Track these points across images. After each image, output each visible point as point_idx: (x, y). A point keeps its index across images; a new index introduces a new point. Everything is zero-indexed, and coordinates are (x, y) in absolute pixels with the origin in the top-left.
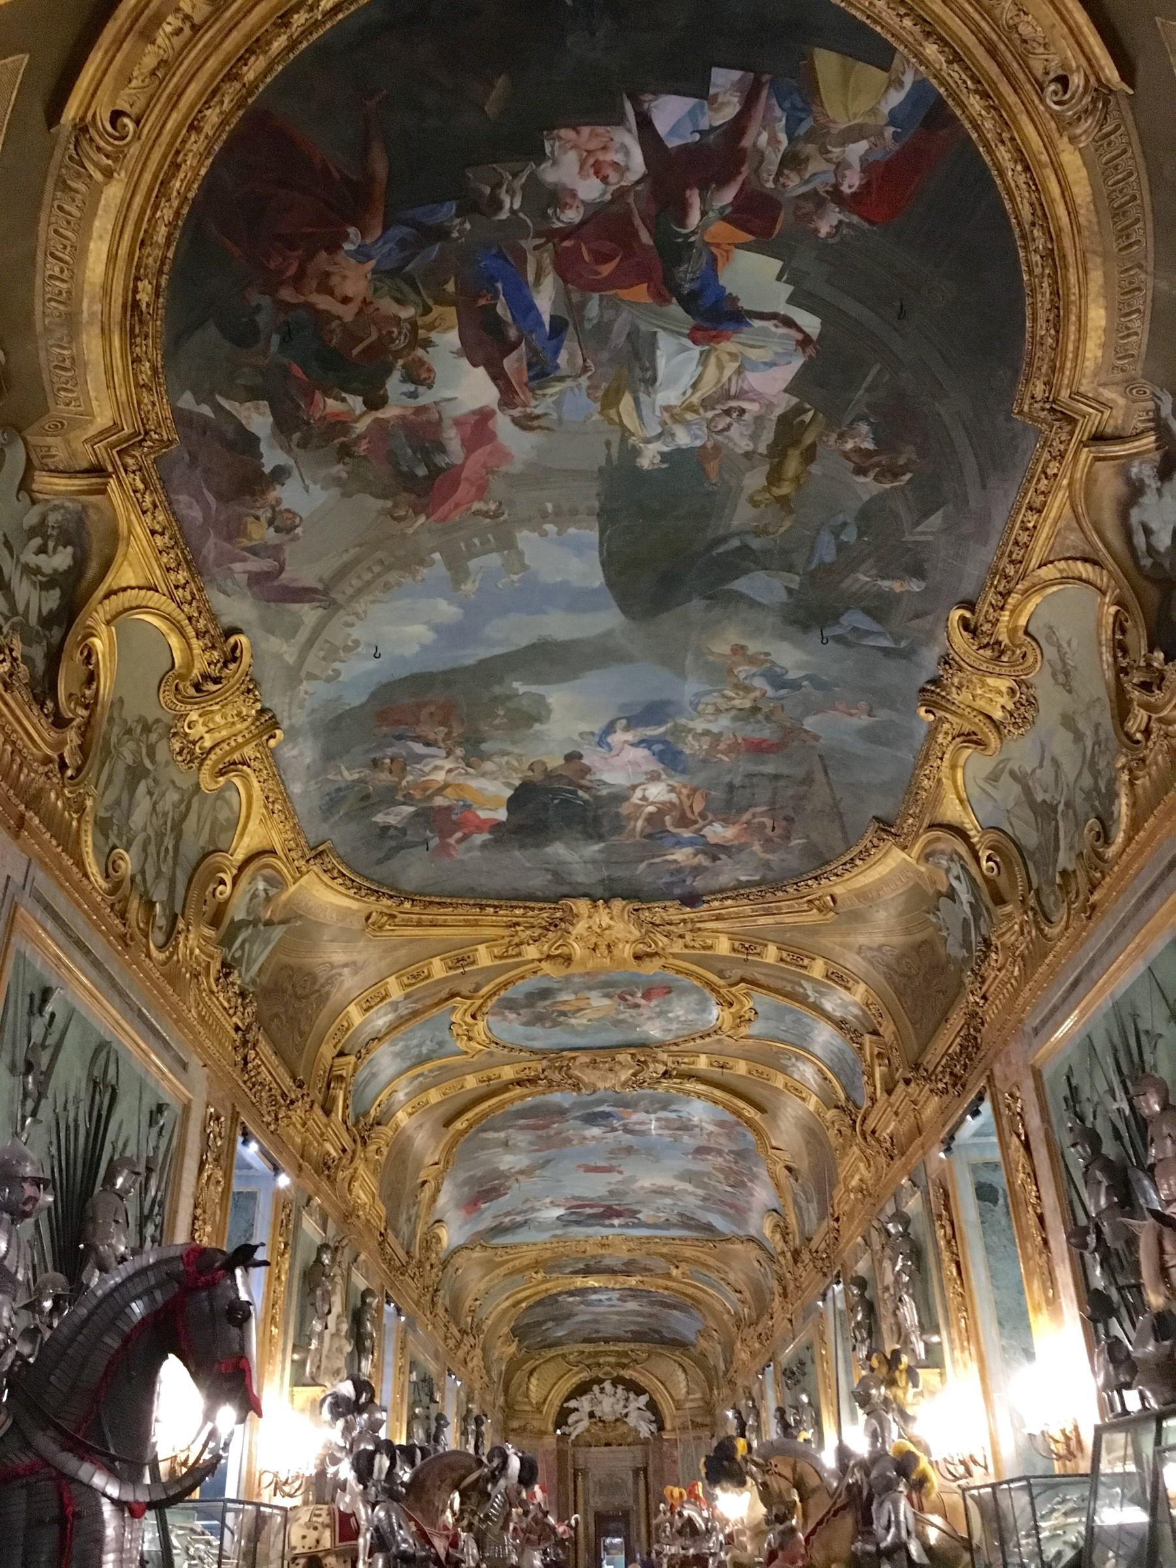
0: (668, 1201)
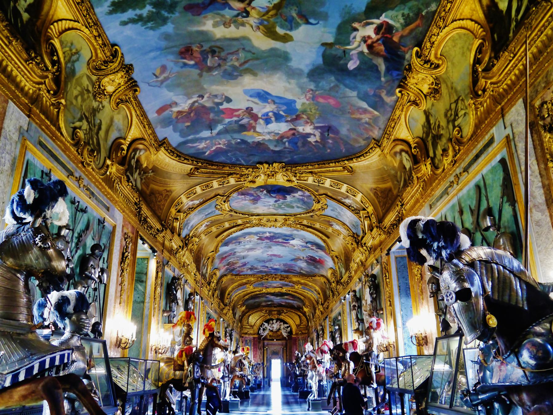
0: (247, 247)
